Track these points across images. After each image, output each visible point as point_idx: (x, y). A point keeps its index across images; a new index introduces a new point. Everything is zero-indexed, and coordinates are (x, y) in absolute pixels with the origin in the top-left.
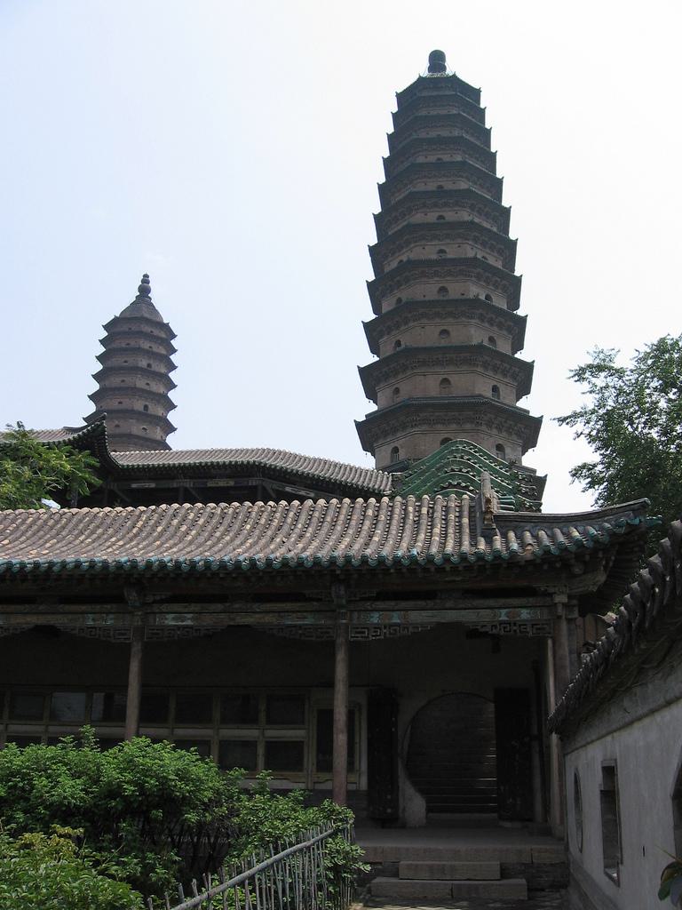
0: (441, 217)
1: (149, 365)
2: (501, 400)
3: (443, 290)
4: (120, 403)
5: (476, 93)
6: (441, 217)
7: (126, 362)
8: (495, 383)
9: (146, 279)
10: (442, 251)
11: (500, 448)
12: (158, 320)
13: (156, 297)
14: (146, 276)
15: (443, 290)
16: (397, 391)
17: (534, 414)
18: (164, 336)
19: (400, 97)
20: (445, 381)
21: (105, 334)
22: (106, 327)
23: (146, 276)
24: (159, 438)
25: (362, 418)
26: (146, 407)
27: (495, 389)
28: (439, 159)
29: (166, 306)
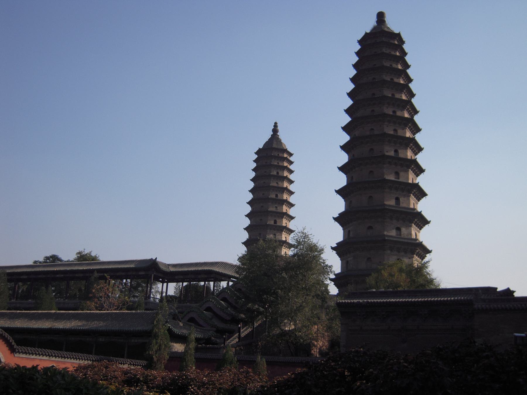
0: (373, 111)
1: (278, 173)
2: (402, 205)
3: (372, 149)
4: (263, 194)
5: (399, 35)
6: (373, 111)
7: (265, 172)
8: (397, 196)
9: (276, 125)
10: (372, 129)
11: (398, 229)
12: (282, 148)
13: (281, 135)
14: (276, 123)
15: (372, 149)
16: (351, 201)
17: (419, 211)
18: (285, 156)
19: (360, 42)
20: (371, 197)
21: (257, 156)
22: (256, 153)
23: (276, 123)
24: (284, 211)
25: (336, 215)
26: (277, 196)
27: (397, 199)
28: (374, 78)
29: (287, 139)
